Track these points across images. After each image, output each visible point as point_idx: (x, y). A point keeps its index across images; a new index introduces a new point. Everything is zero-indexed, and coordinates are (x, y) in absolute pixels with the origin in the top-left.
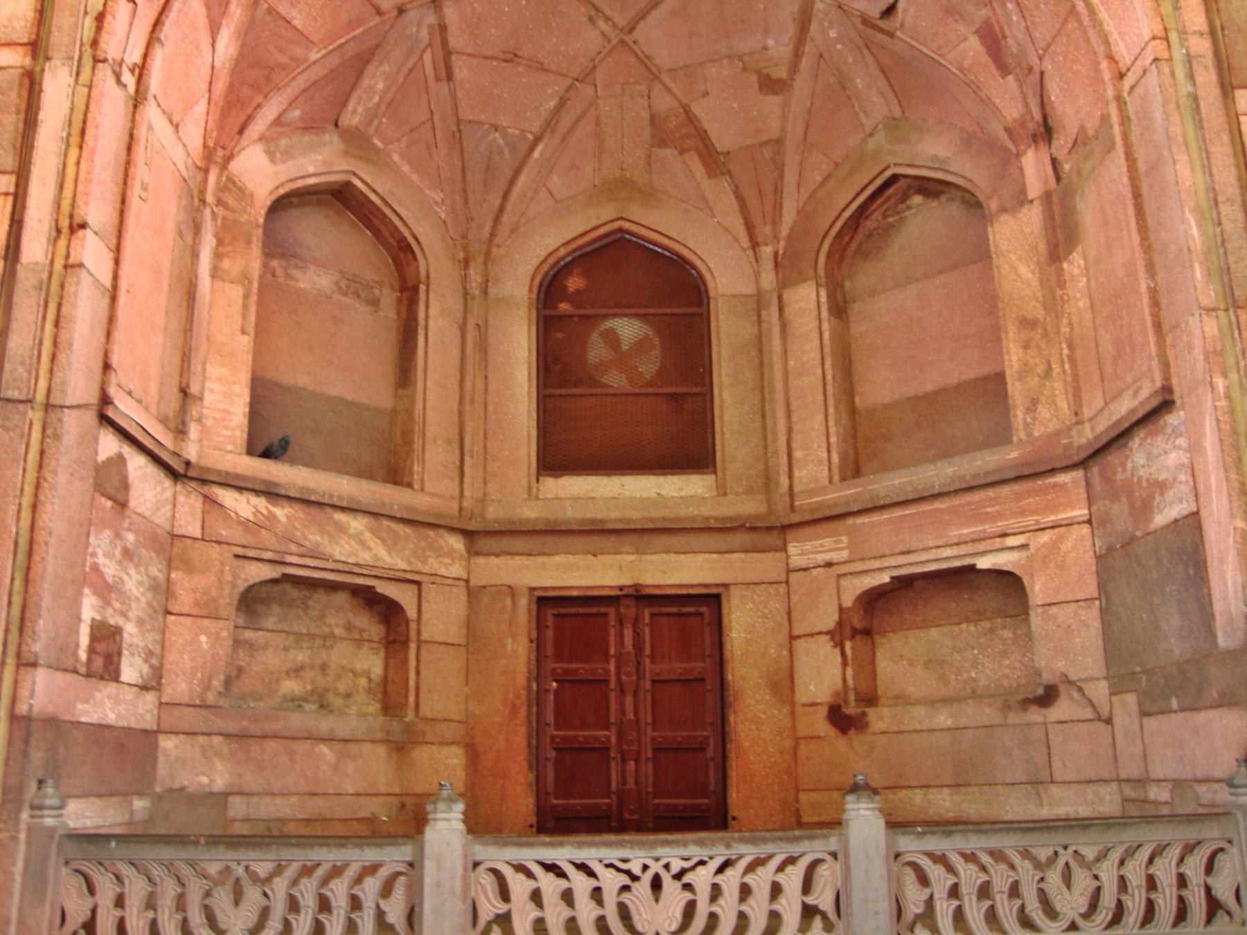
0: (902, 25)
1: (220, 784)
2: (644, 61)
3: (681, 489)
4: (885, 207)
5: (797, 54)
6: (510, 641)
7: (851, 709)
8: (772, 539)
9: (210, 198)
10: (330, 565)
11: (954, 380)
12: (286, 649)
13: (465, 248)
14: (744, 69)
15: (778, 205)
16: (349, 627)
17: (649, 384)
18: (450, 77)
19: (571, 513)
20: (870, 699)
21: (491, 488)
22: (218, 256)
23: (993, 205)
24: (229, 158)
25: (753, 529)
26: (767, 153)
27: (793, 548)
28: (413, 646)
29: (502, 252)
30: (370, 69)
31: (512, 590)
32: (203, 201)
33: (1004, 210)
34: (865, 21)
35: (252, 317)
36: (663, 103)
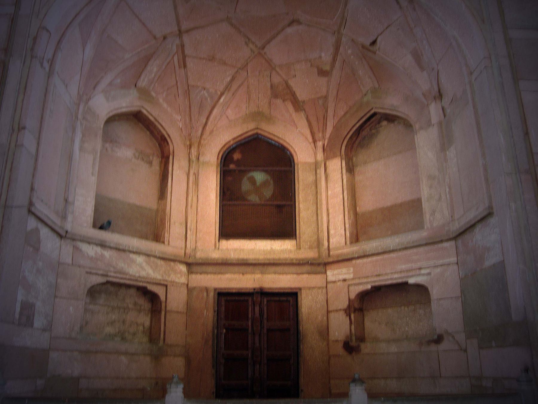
0: (379, 48)
1: (76, 373)
2: (269, 62)
3: (281, 246)
4: (371, 125)
5: (334, 60)
6: (206, 311)
7: (353, 343)
8: (320, 269)
9: (80, 116)
10: (128, 277)
11: (399, 201)
12: (107, 313)
13: (190, 140)
14: (311, 65)
15: (325, 125)
16: (135, 304)
17: (268, 200)
18: (185, 66)
19: (233, 256)
20: (362, 339)
21: (199, 244)
22: (82, 141)
23: (417, 126)
24: (89, 99)
25: (312, 264)
26: (321, 102)
27: (329, 273)
28: (163, 313)
29: (206, 142)
30: (151, 62)
31: (207, 290)
32: (77, 117)
33: (421, 128)
34: (363, 47)
35: (97, 168)
36: (276, 80)
